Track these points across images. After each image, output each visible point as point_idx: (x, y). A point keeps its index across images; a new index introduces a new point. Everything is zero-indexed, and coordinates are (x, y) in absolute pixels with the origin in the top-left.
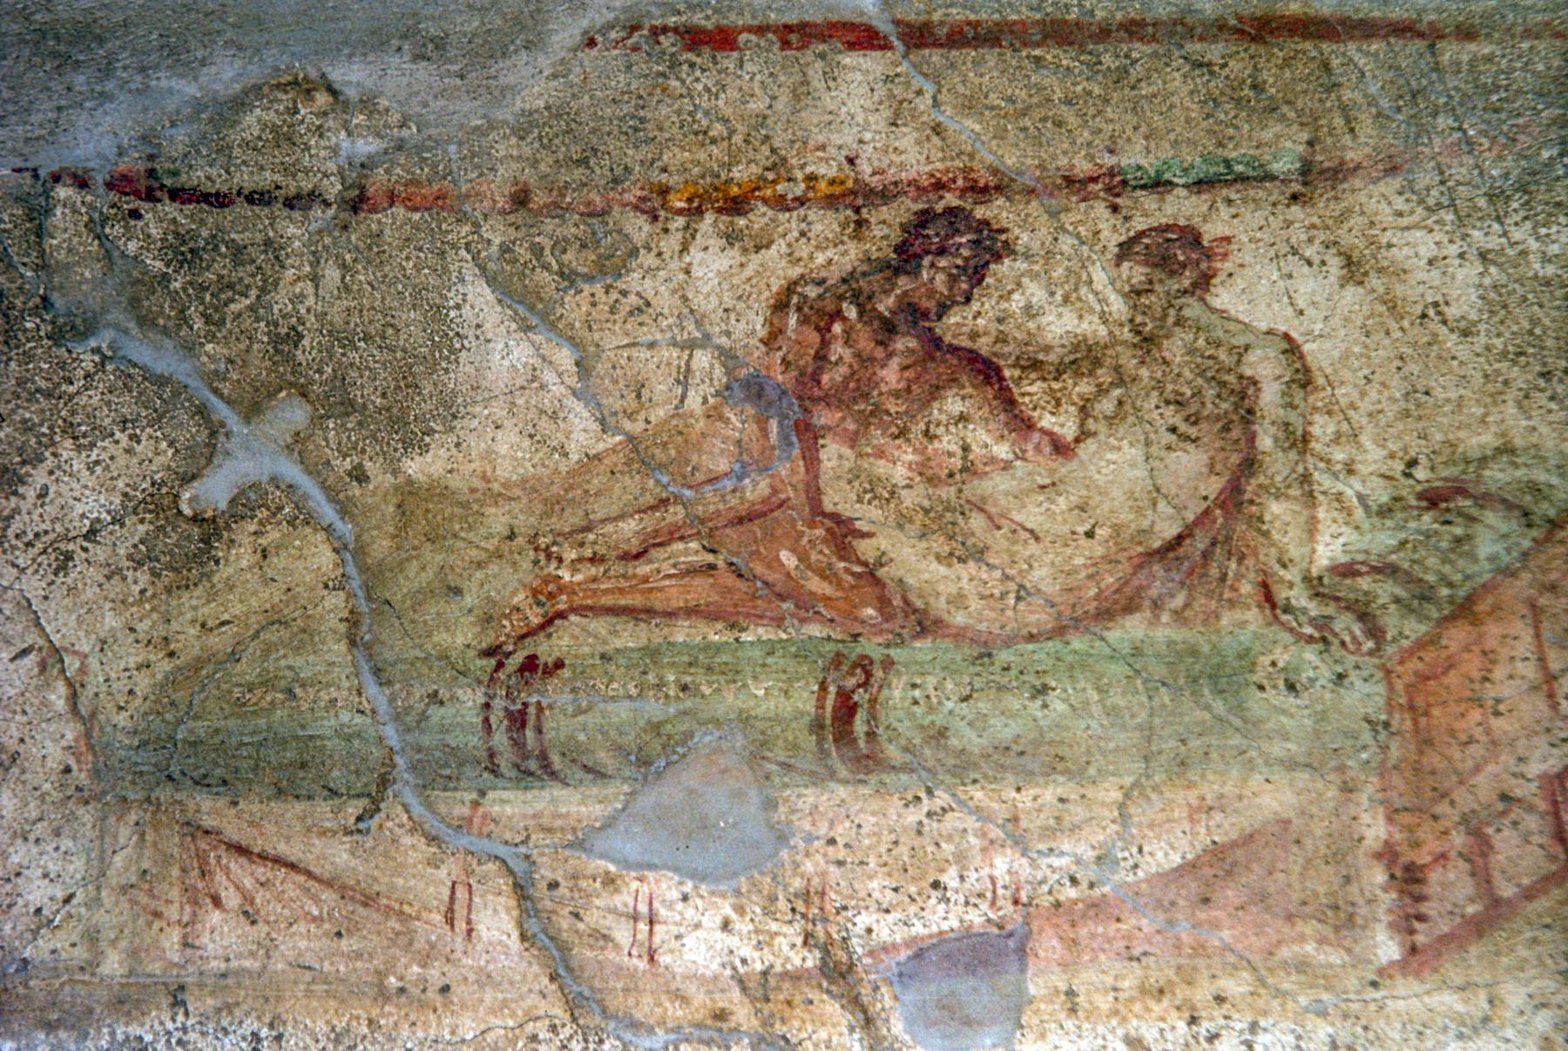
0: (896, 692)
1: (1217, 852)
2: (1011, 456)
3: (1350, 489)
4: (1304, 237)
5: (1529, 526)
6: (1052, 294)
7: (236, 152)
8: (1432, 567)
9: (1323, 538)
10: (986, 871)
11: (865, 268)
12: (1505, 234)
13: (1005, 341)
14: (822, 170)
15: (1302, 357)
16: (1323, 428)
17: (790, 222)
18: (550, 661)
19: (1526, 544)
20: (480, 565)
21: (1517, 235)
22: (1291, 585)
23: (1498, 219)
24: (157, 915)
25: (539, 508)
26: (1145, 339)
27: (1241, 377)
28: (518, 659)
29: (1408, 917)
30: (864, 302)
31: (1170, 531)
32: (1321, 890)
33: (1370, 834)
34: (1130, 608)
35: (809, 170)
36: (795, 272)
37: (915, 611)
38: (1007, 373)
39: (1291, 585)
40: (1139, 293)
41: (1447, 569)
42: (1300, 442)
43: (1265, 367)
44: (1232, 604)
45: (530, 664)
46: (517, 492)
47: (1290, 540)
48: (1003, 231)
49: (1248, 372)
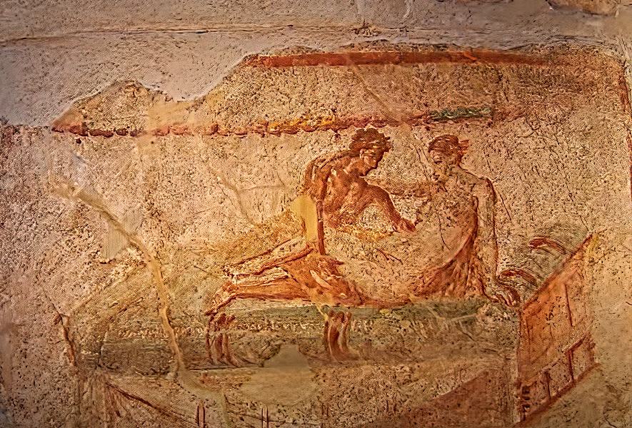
2: (392, 230)
5: (565, 253)
6: (406, 164)
7: (114, 113)
11: (339, 154)
14: (323, 115)
16: (500, 217)
17: (313, 136)
26: (440, 182)
27: (472, 196)
28: (219, 315)
29: (524, 406)
32: (496, 398)
35: (318, 115)
36: (314, 157)
37: (359, 294)
43: (481, 194)
44: (469, 287)
46: (217, 249)
47: (489, 261)
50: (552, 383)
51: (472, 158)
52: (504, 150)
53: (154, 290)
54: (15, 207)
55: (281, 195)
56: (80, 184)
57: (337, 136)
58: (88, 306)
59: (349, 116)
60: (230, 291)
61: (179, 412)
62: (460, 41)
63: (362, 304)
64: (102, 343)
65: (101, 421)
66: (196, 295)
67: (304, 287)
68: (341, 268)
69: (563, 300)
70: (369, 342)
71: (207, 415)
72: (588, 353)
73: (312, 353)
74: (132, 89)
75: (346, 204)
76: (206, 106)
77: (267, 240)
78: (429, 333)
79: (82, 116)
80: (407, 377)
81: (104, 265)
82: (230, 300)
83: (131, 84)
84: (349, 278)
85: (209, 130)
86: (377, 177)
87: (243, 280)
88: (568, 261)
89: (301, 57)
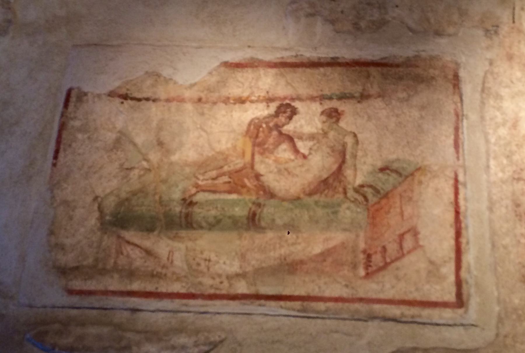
0: (265, 210)
8: (379, 186)
16: (360, 153)
17: (254, 106)
21: (405, 111)
30: (267, 123)
31: (325, 176)
36: (253, 116)
38: (296, 140)
42: (354, 156)
43: (349, 140)
47: (350, 178)
49: (345, 140)
50: (388, 254)
52: (366, 117)
55: (232, 136)
56: (119, 125)
59: (276, 95)
60: (197, 188)
67: (239, 188)
68: (262, 178)
69: (398, 204)
70: (273, 220)
73: (240, 224)
76: (196, 88)
78: (310, 217)
84: (266, 184)
88: (403, 181)
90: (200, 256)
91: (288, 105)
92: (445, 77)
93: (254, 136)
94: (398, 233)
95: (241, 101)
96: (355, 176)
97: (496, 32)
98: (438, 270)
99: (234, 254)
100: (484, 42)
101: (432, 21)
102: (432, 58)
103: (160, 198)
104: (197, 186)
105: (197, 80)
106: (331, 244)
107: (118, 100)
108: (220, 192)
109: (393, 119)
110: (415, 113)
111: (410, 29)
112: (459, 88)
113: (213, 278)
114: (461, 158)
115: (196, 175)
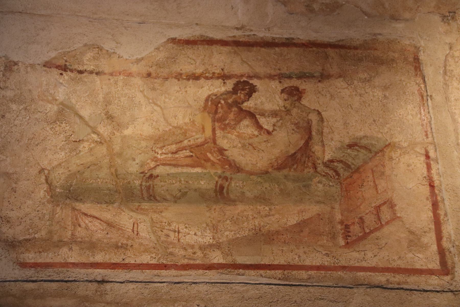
1: (304, 221)
3: (333, 144)
4: (321, 90)
6: (267, 100)
7: (85, 61)
8: (350, 161)
9: (326, 154)
10: (253, 224)
11: (226, 92)
12: (365, 91)
13: (257, 110)
14: (216, 72)
15: (321, 115)
16: (326, 130)
17: (210, 82)
18: (156, 175)
19: (371, 156)
20: (140, 154)
21: (367, 91)
22: (320, 164)
23: (364, 88)
24: (66, 228)
25: (153, 142)
26: (288, 110)
27: (308, 119)
28: (148, 175)
29: (346, 236)
31: (293, 152)
32: (327, 230)
33: (338, 218)
34: (284, 168)
35: (213, 71)
36: (210, 93)
37: (237, 167)
38: (257, 116)
39: (320, 164)
40: (286, 100)
41: (353, 162)
42: (321, 133)
43: (314, 118)
44: (306, 167)
45: (151, 176)
47: (319, 154)
48: (256, 86)
49: (310, 118)
50: (366, 225)
51: (308, 99)
52: (328, 95)
53: (108, 157)
54: (14, 107)
55: (189, 111)
57: (224, 83)
58: (63, 164)
60: (156, 161)
61: (121, 225)
62: (301, 35)
63: (239, 172)
64: (71, 186)
65: (67, 230)
66: (134, 163)
67: (203, 162)
68: (226, 153)
69: (371, 178)
70: (243, 193)
71: (139, 227)
72: (391, 209)
74: (97, 49)
75: (230, 118)
76: (143, 63)
77: (180, 135)
78: (281, 190)
79: (64, 61)
80: (268, 213)
81: (75, 143)
82: (155, 167)
83: (96, 46)
84: (230, 158)
85: (145, 75)
86: (249, 105)
87: (164, 156)
89: (203, 41)
90: (168, 227)
91: (246, 83)
92: (406, 59)
93: (213, 112)
94: (373, 205)
95: (196, 78)
96: (324, 152)
97: (453, 18)
98: (419, 239)
99: (204, 225)
100: (442, 28)
101: (387, 5)
102: (390, 42)
103: (116, 170)
104: (155, 159)
105: (143, 55)
106: (307, 216)
107: (56, 72)
108: (182, 166)
109: (358, 98)
110: (379, 93)
111: (365, 13)
112: (420, 70)
113: (185, 249)
114: (430, 136)
115: (154, 149)
